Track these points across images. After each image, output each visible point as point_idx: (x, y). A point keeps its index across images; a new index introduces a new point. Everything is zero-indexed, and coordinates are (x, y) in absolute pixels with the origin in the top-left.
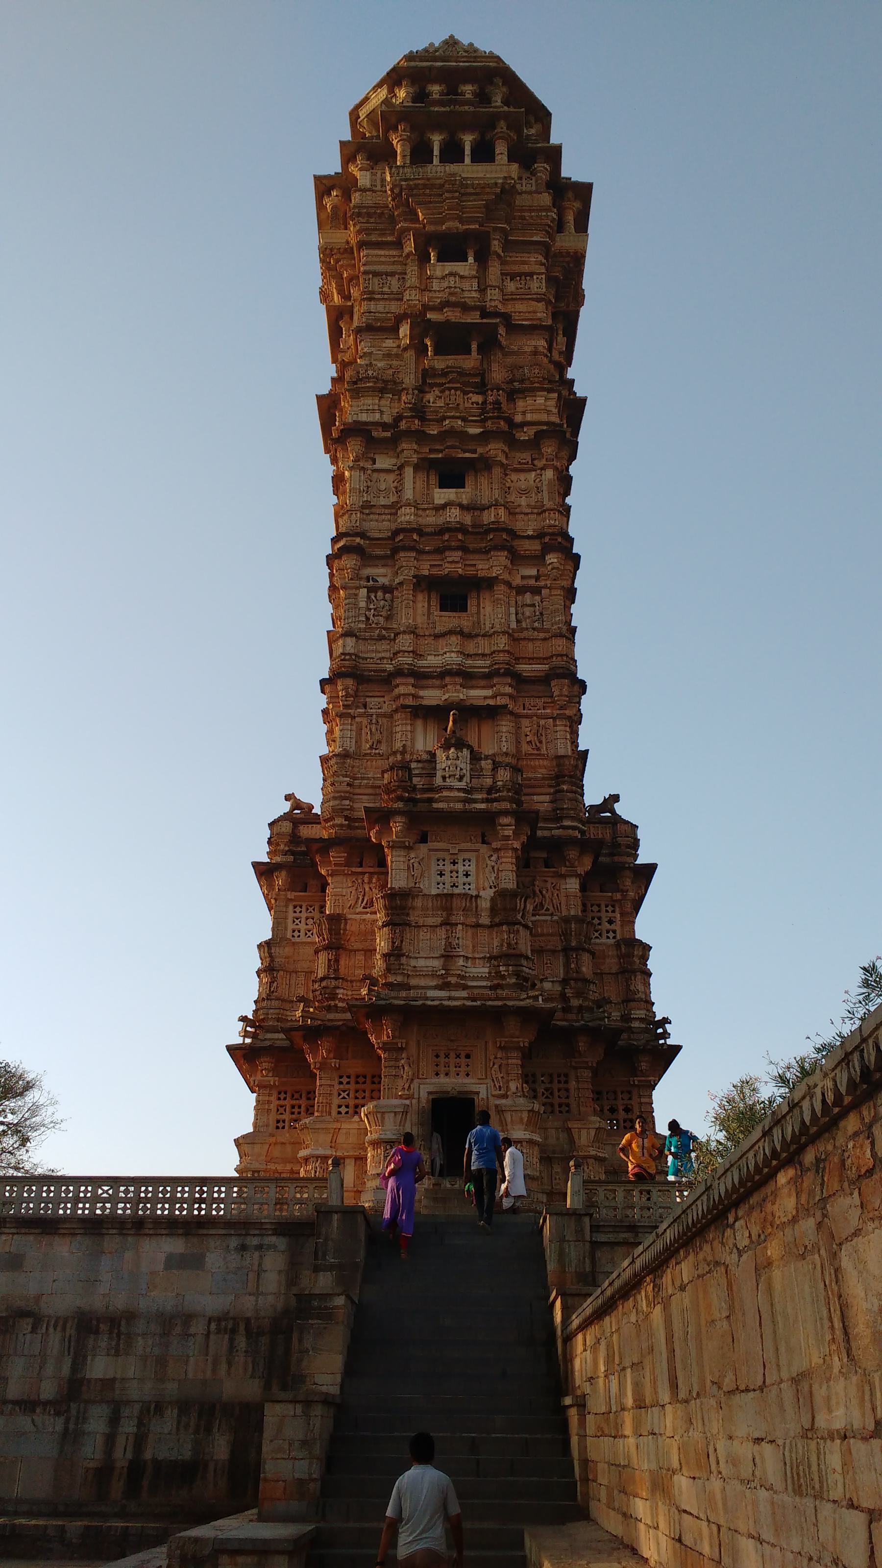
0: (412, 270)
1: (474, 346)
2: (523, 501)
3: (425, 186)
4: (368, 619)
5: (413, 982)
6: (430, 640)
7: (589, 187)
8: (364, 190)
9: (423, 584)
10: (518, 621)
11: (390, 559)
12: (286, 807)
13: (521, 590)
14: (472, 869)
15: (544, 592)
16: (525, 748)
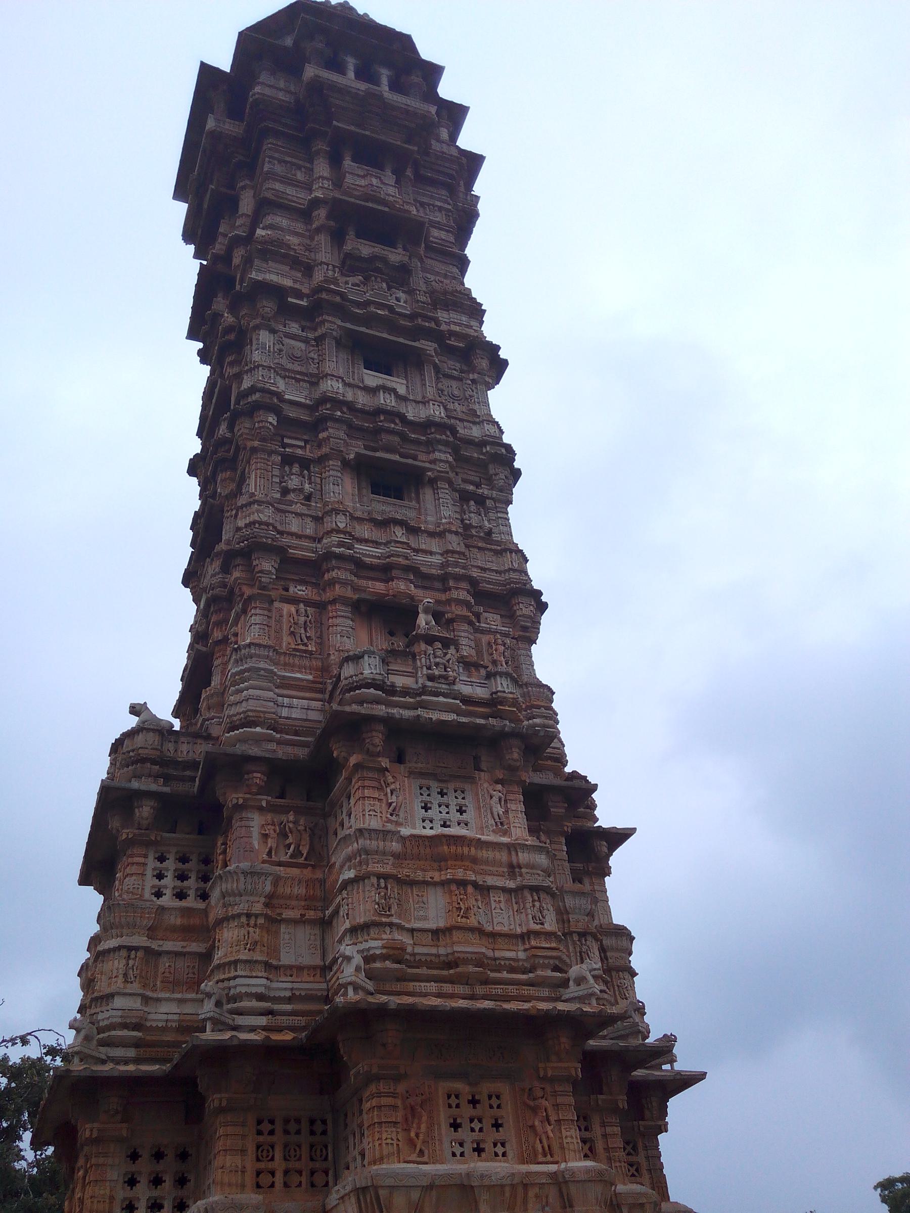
12: (132, 722)
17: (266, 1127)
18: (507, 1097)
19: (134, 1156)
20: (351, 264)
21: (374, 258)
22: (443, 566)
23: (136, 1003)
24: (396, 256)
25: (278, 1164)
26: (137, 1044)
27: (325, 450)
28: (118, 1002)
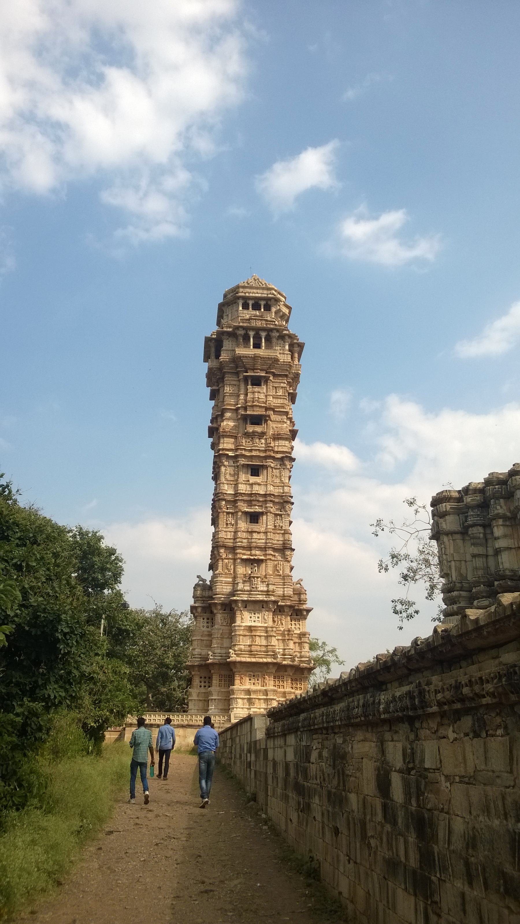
1: (263, 422)
13: (276, 515)
17: (221, 676)
18: (260, 675)
19: (201, 678)
20: (247, 435)
21: (254, 432)
22: (266, 543)
23: (200, 650)
25: (223, 682)
26: (200, 658)
28: (196, 650)
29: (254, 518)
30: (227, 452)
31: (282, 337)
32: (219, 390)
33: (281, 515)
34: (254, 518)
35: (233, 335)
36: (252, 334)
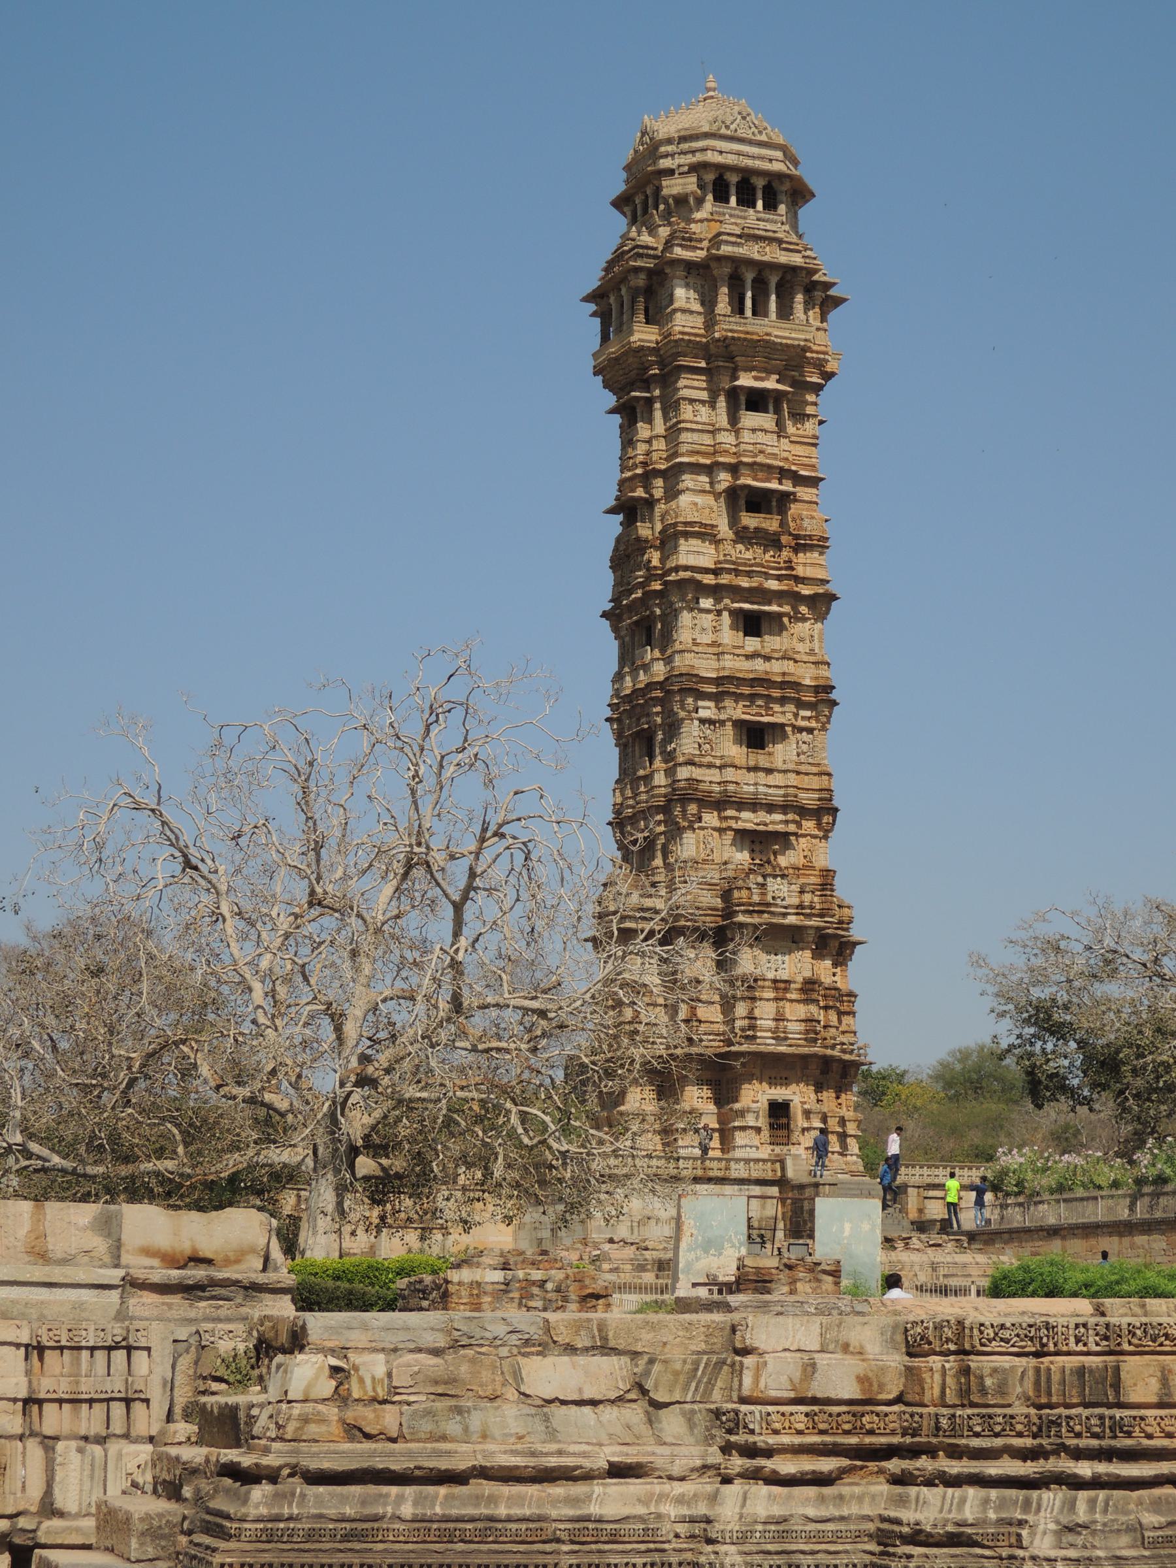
0: (722, 403)
1: (774, 504)
2: (800, 647)
3: (745, 339)
4: (700, 746)
5: (759, 1034)
6: (744, 771)
7: (845, 300)
8: (684, 311)
9: (739, 724)
10: (798, 755)
11: (717, 698)
13: (801, 730)
14: (787, 962)
15: (816, 732)
16: (803, 861)
20: (743, 536)
24: (771, 524)
27: (723, 717)
29: (756, 736)
30: (698, 576)
31: (811, 288)
32: (649, 402)
33: (810, 731)
34: (756, 736)
35: (701, 274)
36: (749, 276)
